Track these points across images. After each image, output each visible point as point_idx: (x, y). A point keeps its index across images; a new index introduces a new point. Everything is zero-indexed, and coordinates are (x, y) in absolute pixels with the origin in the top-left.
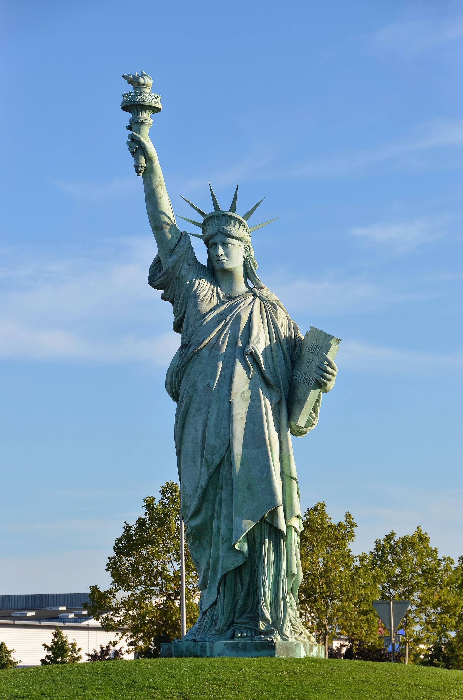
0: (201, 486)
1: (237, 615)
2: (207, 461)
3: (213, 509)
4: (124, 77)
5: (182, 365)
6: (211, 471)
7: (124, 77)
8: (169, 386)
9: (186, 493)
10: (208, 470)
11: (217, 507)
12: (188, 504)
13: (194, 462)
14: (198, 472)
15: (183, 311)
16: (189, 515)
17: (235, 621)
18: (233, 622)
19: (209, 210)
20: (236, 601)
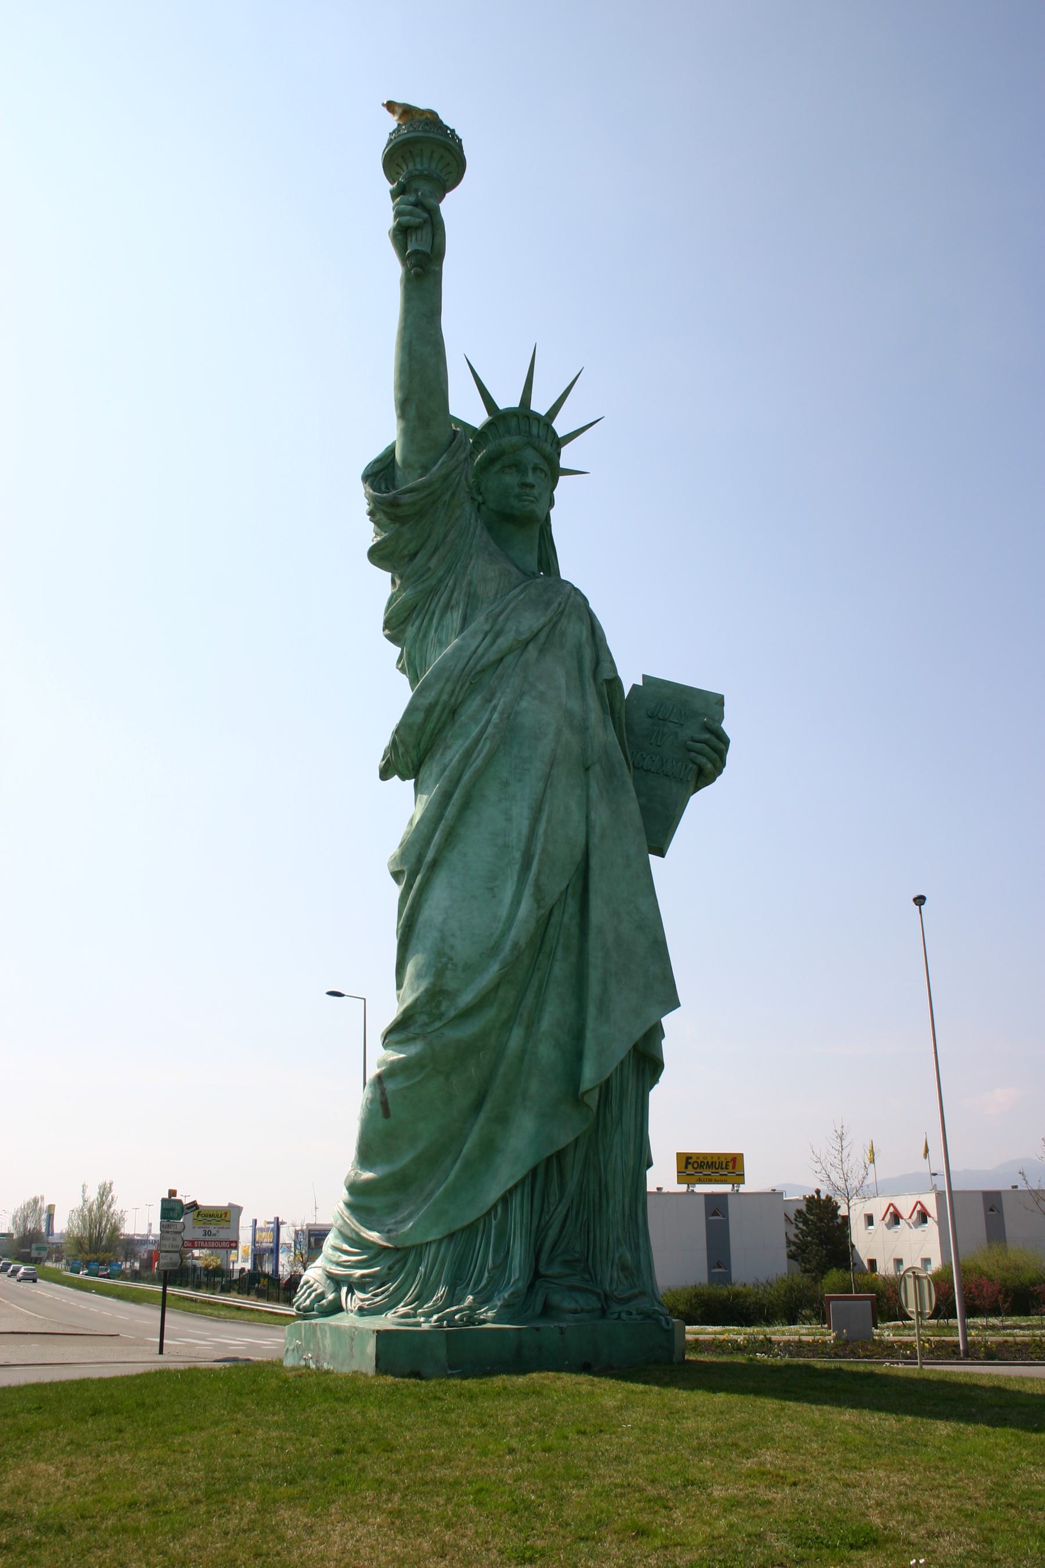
0: (515, 945)
1: (544, 1257)
2: (538, 887)
3: (518, 1004)
4: (390, 106)
5: (478, 667)
6: (543, 911)
7: (390, 106)
8: (420, 716)
9: (450, 959)
10: (539, 907)
11: (530, 999)
12: (451, 983)
13: (491, 889)
14: (504, 912)
15: (440, 573)
16: (452, 1013)
17: (542, 1270)
18: (537, 1275)
19: (507, 399)
20: (543, 1222)
